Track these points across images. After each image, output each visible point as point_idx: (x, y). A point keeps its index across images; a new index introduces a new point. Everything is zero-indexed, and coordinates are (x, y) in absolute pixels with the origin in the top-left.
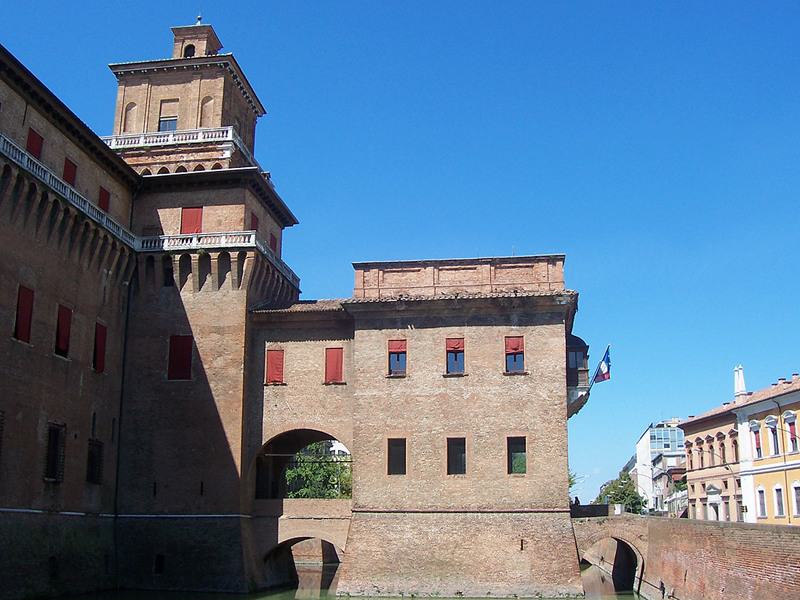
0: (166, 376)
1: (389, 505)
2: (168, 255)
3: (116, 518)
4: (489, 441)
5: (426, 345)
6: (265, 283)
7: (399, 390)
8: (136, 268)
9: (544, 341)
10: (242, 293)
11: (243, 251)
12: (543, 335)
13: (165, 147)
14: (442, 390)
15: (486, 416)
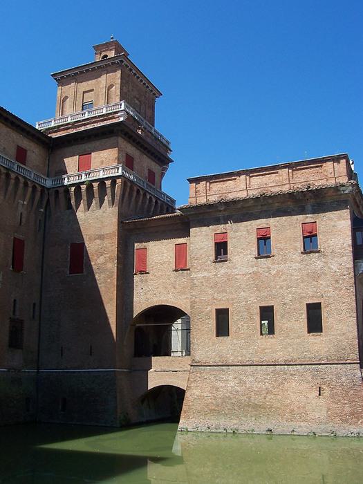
0: (68, 272)
1: (218, 361)
2: (67, 188)
3: (38, 372)
4: (292, 307)
5: (242, 235)
6: (137, 202)
7: (223, 271)
8: (48, 200)
9: (333, 223)
10: (115, 209)
11: (114, 179)
12: (332, 220)
13: (83, 120)
14: (255, 268)
15: (289, 287)
